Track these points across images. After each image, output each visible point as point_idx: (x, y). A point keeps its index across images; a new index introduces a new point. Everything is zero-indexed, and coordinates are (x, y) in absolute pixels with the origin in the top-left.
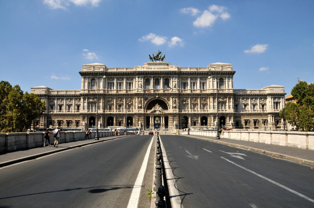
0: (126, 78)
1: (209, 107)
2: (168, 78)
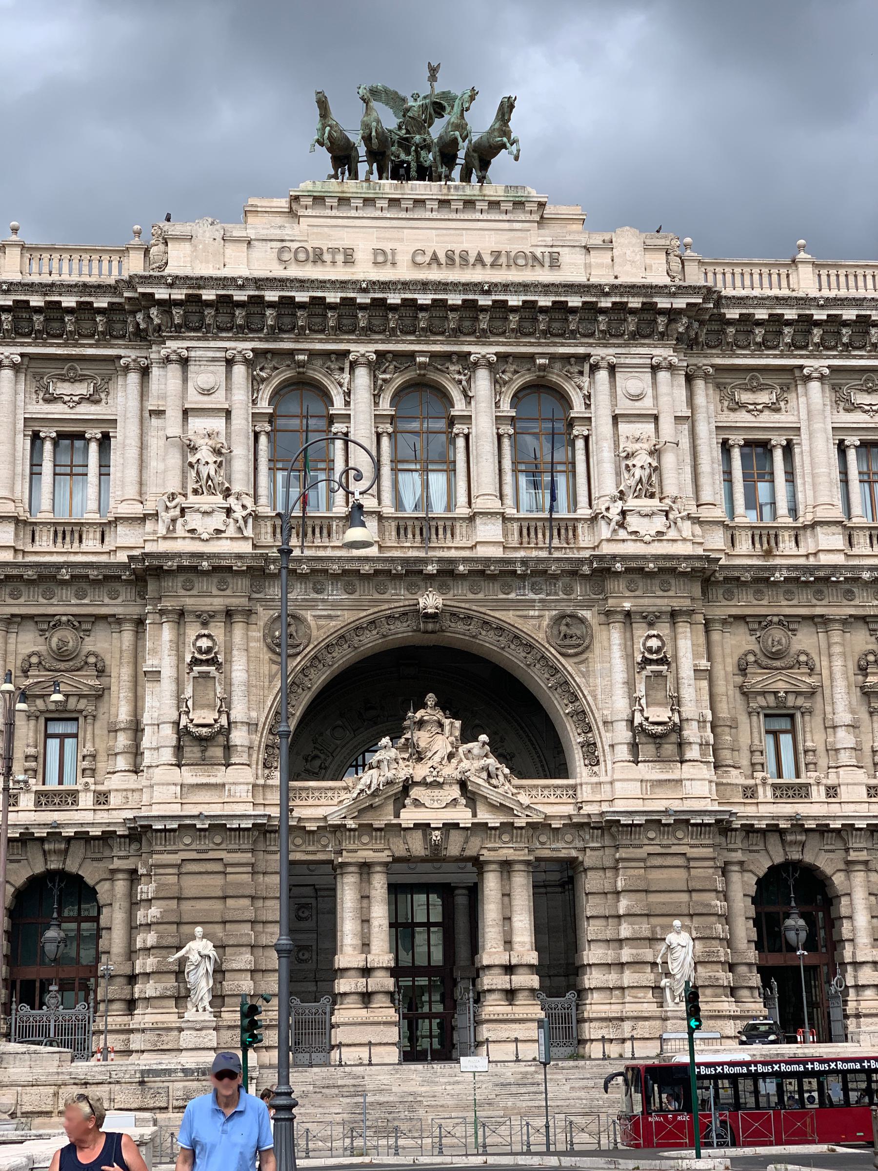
0: (16, 368)
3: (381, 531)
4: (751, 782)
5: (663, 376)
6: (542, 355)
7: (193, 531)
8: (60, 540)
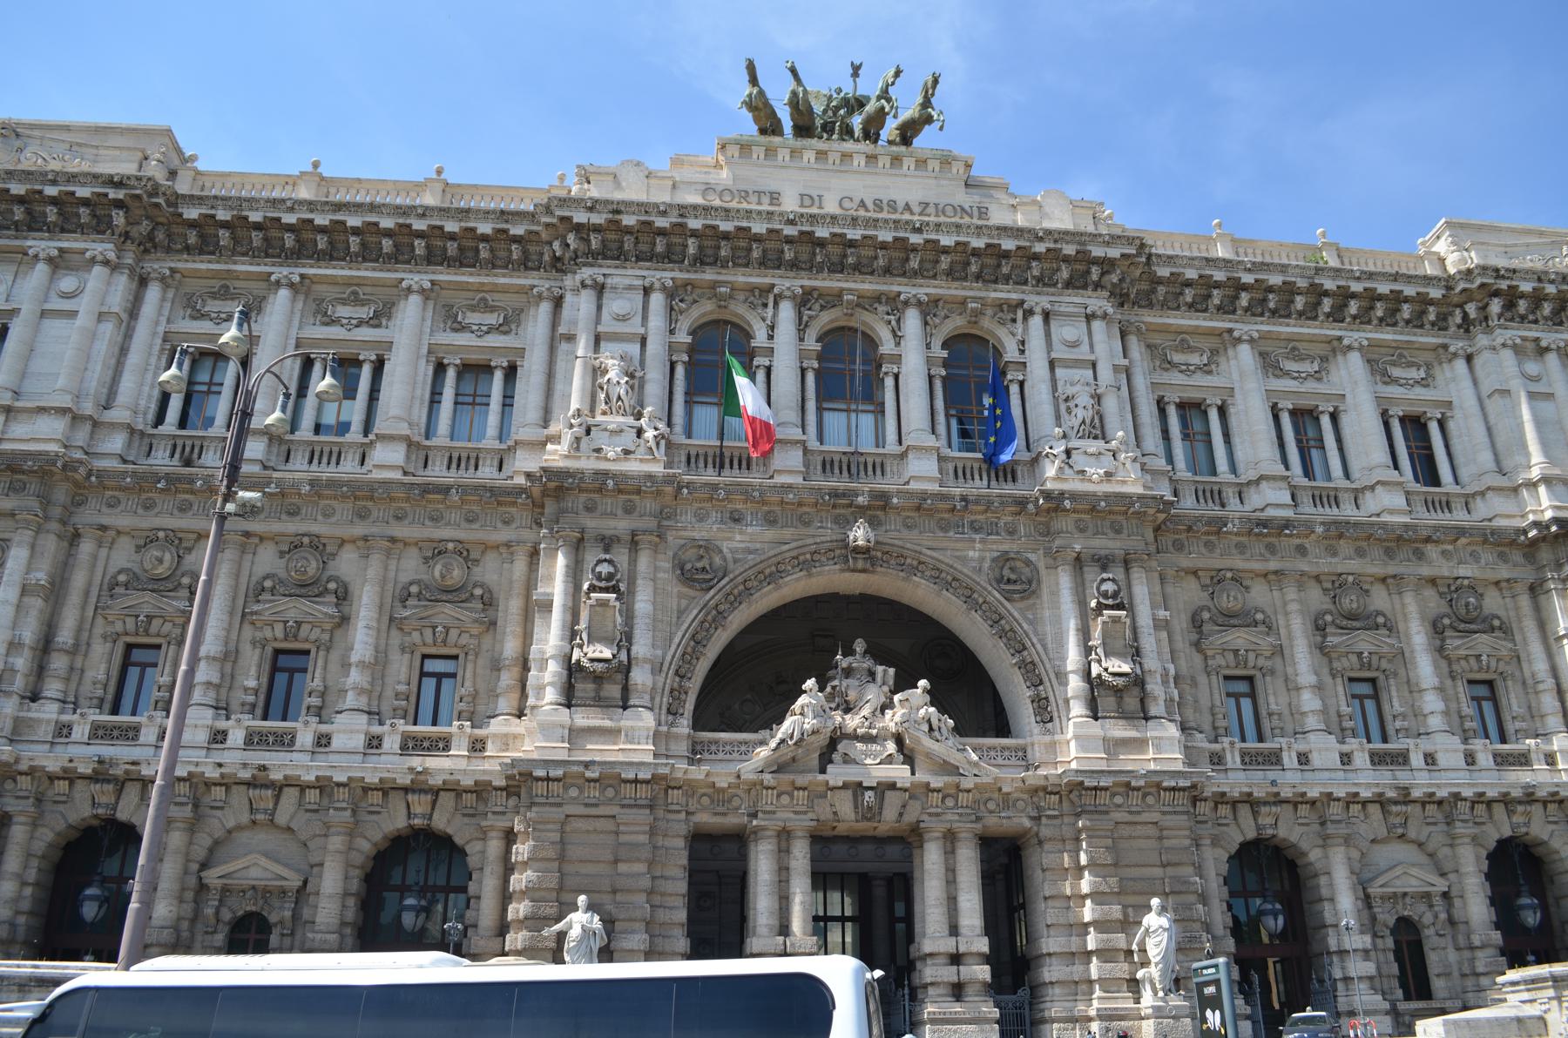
1: (1549, 702)
2: (987, 323)
3: (807, 464)
4: (1217, 747)
5: (1097, 325)
6: (975, 299)
7: (598, 450)
8: (454, 465)
